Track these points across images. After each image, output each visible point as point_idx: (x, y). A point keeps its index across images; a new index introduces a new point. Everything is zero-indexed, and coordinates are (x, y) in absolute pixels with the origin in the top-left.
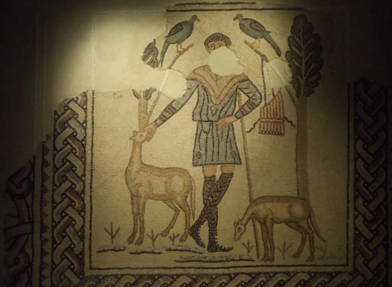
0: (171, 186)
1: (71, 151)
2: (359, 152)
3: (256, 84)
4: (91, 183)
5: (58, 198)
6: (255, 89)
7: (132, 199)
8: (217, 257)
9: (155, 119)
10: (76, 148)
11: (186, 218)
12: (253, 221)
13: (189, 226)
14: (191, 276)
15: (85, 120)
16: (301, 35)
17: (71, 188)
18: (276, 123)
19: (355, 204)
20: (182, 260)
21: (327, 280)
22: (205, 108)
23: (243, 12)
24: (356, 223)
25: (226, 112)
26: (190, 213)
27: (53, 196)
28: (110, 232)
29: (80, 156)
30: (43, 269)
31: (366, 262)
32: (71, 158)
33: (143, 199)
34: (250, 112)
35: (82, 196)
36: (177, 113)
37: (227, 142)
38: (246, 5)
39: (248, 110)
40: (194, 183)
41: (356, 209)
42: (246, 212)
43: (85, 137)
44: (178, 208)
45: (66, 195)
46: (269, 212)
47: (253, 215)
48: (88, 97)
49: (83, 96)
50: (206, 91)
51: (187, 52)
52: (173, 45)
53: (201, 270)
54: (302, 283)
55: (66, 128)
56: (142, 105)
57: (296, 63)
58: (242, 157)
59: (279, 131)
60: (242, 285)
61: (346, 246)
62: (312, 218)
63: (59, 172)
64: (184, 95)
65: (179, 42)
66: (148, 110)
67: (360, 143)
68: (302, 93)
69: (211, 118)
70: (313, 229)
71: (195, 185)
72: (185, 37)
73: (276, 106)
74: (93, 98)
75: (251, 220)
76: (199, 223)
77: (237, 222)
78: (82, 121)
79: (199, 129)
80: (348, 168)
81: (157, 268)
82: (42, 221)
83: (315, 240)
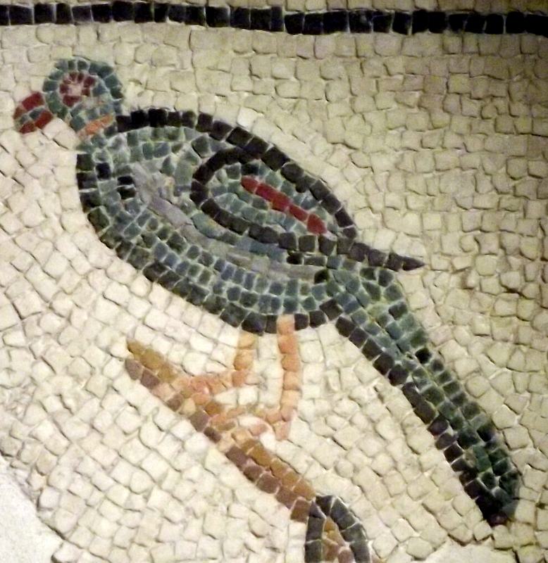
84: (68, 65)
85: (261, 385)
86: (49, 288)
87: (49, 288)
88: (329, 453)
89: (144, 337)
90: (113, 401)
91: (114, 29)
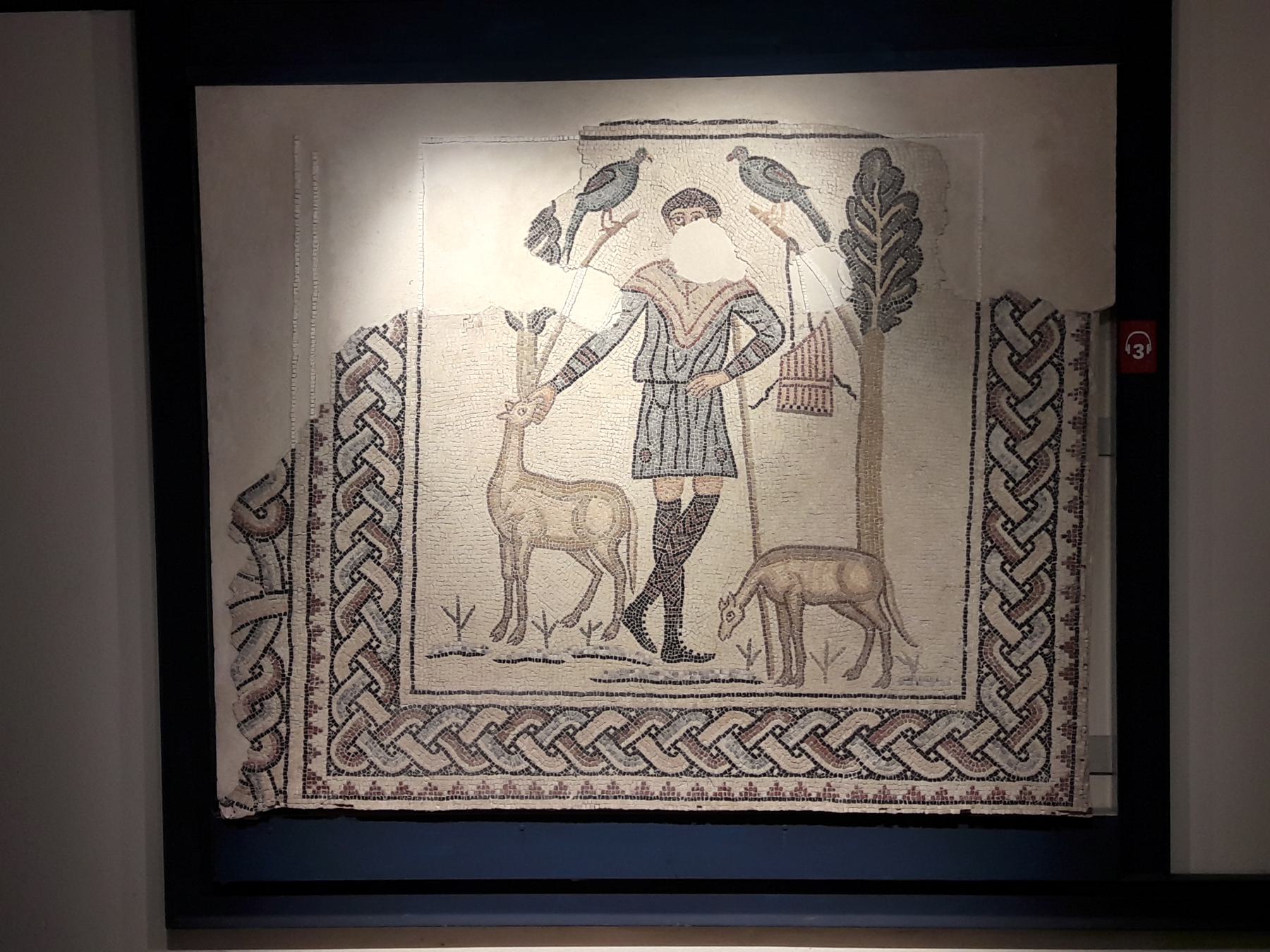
1: (373, 442)
3: (773, 305)
4: (415, 511)
5: (343, 544)
6: (771, 313)
7: (501, 546)
8: (680, 673)
10: (384, 435)
11: (616, 588)
12: (759, 596)
16: (875, 195)
17: (373, 521)
18: (813, 389)
19: (983, 568)
20: (606, 677)
21: (917, 729)
22: (661, 352)
23: (748, 143)
24: (984, 607)
25: (707, 363)
27: (333, 535)
28: (455, 615)
30: (312, 689)
31: (1003, 692)
32: (372, 455)
33: (525, 546)
34: (758, 364)
35: (396, 537)
36: (600, 364)
37: (707, 427)
39: (756, 360)
40: (635, 514)
42: (745, 579)
43: (401, 412)
44: (600, 566)
45: (361, 534)
47: (761, 586)
49: (398, 322)
50: (663, 316)
52: (594, 213)
53: (645, 699)
54: (864, 732)
55: (360, 391)
58: (740, 461)
59: (820, 406)
60: (733, 734)
61: (961, 657)
63: (346, 485)
64: (615, 325)
66: (539, 356)
67: (999, 434)
68: (874, 326)
70: (889, 618)
71: (636, 520)
73: (817, 352)
74: (420, 327)
75: (756, 596)
76: (644, 601)
77: (725, 599)
78: (395, 378)
80: (971, 489)
84: (737, 147)
85: (777, 213)
86: (734, 194)
87: (734, 194)
89: (753, 204)
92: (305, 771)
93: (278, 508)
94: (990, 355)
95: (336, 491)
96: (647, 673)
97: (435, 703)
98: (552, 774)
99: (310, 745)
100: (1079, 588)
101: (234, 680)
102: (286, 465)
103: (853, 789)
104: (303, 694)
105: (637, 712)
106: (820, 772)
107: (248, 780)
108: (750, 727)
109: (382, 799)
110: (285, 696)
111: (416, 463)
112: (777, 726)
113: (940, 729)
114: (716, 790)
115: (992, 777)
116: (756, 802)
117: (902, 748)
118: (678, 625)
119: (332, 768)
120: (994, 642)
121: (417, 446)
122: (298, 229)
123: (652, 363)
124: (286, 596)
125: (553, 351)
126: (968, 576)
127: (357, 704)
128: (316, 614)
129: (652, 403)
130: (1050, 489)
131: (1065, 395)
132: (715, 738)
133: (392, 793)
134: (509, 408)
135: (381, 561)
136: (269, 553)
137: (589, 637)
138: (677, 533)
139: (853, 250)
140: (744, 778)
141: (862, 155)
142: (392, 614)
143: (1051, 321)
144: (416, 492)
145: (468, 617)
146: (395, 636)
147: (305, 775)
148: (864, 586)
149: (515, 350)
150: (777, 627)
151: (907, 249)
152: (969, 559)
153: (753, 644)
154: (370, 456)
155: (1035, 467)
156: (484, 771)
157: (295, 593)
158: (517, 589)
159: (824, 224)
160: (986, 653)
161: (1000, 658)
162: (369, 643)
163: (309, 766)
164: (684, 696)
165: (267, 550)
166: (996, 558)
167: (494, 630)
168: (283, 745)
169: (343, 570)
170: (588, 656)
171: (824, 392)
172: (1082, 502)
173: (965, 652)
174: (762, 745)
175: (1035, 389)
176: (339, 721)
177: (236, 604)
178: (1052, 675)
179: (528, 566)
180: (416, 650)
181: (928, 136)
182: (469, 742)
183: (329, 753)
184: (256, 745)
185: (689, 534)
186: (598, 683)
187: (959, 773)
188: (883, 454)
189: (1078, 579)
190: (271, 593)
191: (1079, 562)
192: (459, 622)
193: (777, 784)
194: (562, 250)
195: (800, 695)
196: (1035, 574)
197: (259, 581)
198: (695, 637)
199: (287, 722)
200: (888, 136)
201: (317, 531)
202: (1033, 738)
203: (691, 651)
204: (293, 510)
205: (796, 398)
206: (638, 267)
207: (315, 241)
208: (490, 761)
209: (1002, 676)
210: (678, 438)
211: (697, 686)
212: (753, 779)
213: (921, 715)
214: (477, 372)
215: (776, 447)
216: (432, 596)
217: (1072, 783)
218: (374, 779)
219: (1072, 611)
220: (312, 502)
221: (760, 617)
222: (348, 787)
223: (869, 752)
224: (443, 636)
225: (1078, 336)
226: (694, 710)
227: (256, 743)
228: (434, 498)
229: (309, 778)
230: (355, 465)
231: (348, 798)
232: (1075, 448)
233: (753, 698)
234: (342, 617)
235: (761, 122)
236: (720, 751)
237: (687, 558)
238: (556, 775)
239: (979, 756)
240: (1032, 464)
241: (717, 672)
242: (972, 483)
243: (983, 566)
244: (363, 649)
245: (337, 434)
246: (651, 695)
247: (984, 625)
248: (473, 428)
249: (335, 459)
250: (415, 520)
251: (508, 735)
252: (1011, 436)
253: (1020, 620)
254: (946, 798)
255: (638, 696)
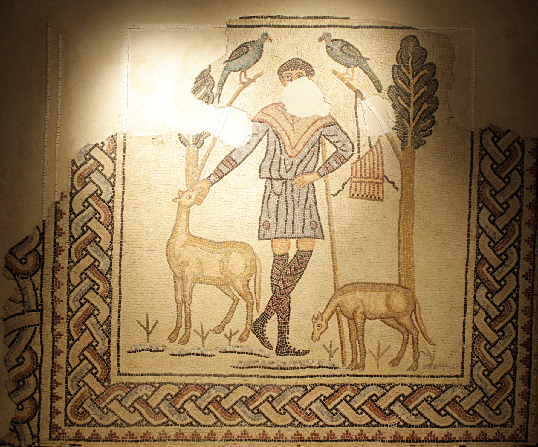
0: (228, 266)
1: (94, 216)
2: (483, 226)
3: (346, 131)
4: (120, 260)
5: (75, 280)
6: (345, 136)
7: (175, 282)
8: (288, 363)
9: (209, 174)
10: (101, 212)
11: (247, 309)
12: (337, 314)
13: (252, 320)
14: (253, 387)
15: (113, 174)
16: (410, 64)
17: (94, 266)
18: (372, 184)
20: (241, 365)
21: (434, 396)
22: (277, 160)
23: (331, 30)
24: (475, 320)
25: (306, 167)
26: (253, 303)
27: (68, 275)
28: (145, 326)
29: (106, 222)
30: (55, 372)
31: (486, 373)
33: (190, 282)
34: (337, 168)
35: (108, 276)
36: (238, 167)
37: (305, 207)
38: (336, 20)
39: (336, 165)
40: (259, 262)
41: (476, 302)
42: (329, 304)
43: (112, 197)
45: (86, 274)
46: (360, 304)
47: (338, 308)
48: (117, 143)
49: (111, 140)
50: (278, 138)
51: (253, 83)
52: (235, 73)
53: (266, 379)
54: (401, 398)
55: (87, 184)
56: (191, 156)
57: (402, 102)
58: (326, 228)
59: (376, 195)
60: (320, 400)
61: (461, 351)
62: (417, 313)
63: (77, 243)
64: (248, 143)
65: (242, 70)
66: (200, 162)
67: (485, 213)
68: (409, 145)
69: (284, 176)
70: (418, 328)
72: (252, 63)
73: (374, 161)
74: (124, 143)
75: (335, 314)
76: (265, 317)
77: (316, 316)
78: (108, 176)
79: (267, 191)
80: (468, 247)
81: (208, 376)
82: (53, 308)
83: (419, 342)
84: (324, 33)
85: (349, 75)
86: (322, 62)
87: (322, 62)
88: (358, 84)
89: (334, 69)
90: (331, 77)
91: (331, 28)
92: (51, 423)
93: (34, 258)
94: (480, 164)
95: (71, 247)
96: (266, 362)
97: (133, 381)
98: (206, 426)
99: (54, 407)
100: (532, 308)
101: (7, 366)
102: (39, 230)
103: (394, 433)
104: (50, 375)
105: (260, 387)
106: (374, 423)
107: (15, 428)
108: (331, 396)
109: (99, 441)
110: (38, 376)
111: (122, 230)
112: (348, 395)
113: (448, 396)
114: (309, 435)
115: (478, 425)
116: (334, 443)
117: (424, 408)
118: (287, 332)
119: (68, 422)
120: (481, 342)
121: (122, 219)
122: (49, 82)
123: (271, 167)
124: (39, 313)
125: (208, 159)
126: (466, 301)
127: (83, 381)
128: (58, 325)
129: (271, 192)
130: (515, 247)
131: (524, 189)
132: (309, 403)
133: (106, 437)
134: (181, 195)
135: (99, 291)
136: (28, 286)
137: (230, 340)
138: (286, 275)
139: (396, 98)
140: (327, 428)
141: (401, 39)
142: (106, 325)
143: (516, 144)
144: (121, 248)
145: (153, 327)
146: (107, 339)
147: (50, 426)
148: (402, 308)
149: (184, 158)
150: (348, 333)
151: (429, 98)
152: (466, 290)
153: (333, 344)
154: (92, 225)
155: (507, 233)
156: (163, 424)
157: (45, 311)
158: (185, 310)
159: (378, 81)
160: (476, 349)
161: (484, 351)
162: (91, 344)
163: (53, 420)
164: (290, 377)
165: (27, 284)
166: (483, 290)
167: (170, 336)
168: (37, 407)
169: (75, 297)
170: (230, 352)
171: (378, 186)
172: (534, 255)
173: (463, 348)
174: (338, 407)
175: (507, 185)
176: (72, 392)
177: (8, 318)
178: (515, 362)
179: (191, 295)
180: (120, 348)
181: (442, 28)
182: (154, 405)
183: (66, 412)
184: (20, 407)
185: (293, 275)
186: (235, 369)
187: (459, 422)
188: (415, 225)
189: (532, 303)
190: (29, 311)
191: (533, 292)
192: (148, 331)
193: (347, 431)
194: (215, 95)
195: (362, 376)
196: (506, 300)
197: (22, 304)
198: (297, 340)
199: (40, 393)
200: (417, 28)
201: (59, 273)
202: (504, 400)
203: (294, 349)
204: (43, 259)
205: (361, 189)
206: (263, 106)
207: (60, 90)
208: (167, 417)
209: (486, 363)
210: (287, 214)
211: (297, 370)
212: (332, 428)
213: (436, 387)
214: (160, 172)
215: (348, 221)
216: (131, 314)
217: (527, 428)
218: (94, 428)
219: (528, 322)
220: (55, 255)
221: (337, 327)
222: (78, 433)
223: (404, 411)
224: (137, 340)
225: (532, 153)
226: (296, 386)
227: (20, 405)
228: (132, 252)
229: (53, 427)
230: (83, 230)
231: (78, 441)
232: (530, 222)
233: (333, 378)
234: (74, 327)
235: (339, 18)
236: (312, 411)
237: (292, 290)
238: (209, 426)
239: (471, 412)
240: (505, 231)
241: (311, 361)
242: (469, 243)
243: (475, 295)
244: (87, 347)
245: (72, 211)
246: (269, 377)
247: (475, 331)
248: (158, 208)
249: (70, 227)
250: (120, 265)
251: (179, 401)
252: (493, 214)
253: (497, 328)
254: (451, 438)
255: (261, 377)
